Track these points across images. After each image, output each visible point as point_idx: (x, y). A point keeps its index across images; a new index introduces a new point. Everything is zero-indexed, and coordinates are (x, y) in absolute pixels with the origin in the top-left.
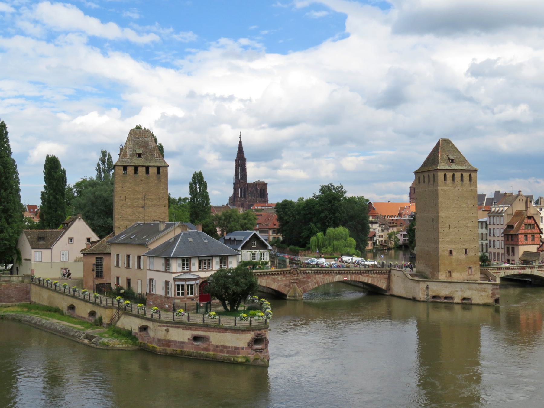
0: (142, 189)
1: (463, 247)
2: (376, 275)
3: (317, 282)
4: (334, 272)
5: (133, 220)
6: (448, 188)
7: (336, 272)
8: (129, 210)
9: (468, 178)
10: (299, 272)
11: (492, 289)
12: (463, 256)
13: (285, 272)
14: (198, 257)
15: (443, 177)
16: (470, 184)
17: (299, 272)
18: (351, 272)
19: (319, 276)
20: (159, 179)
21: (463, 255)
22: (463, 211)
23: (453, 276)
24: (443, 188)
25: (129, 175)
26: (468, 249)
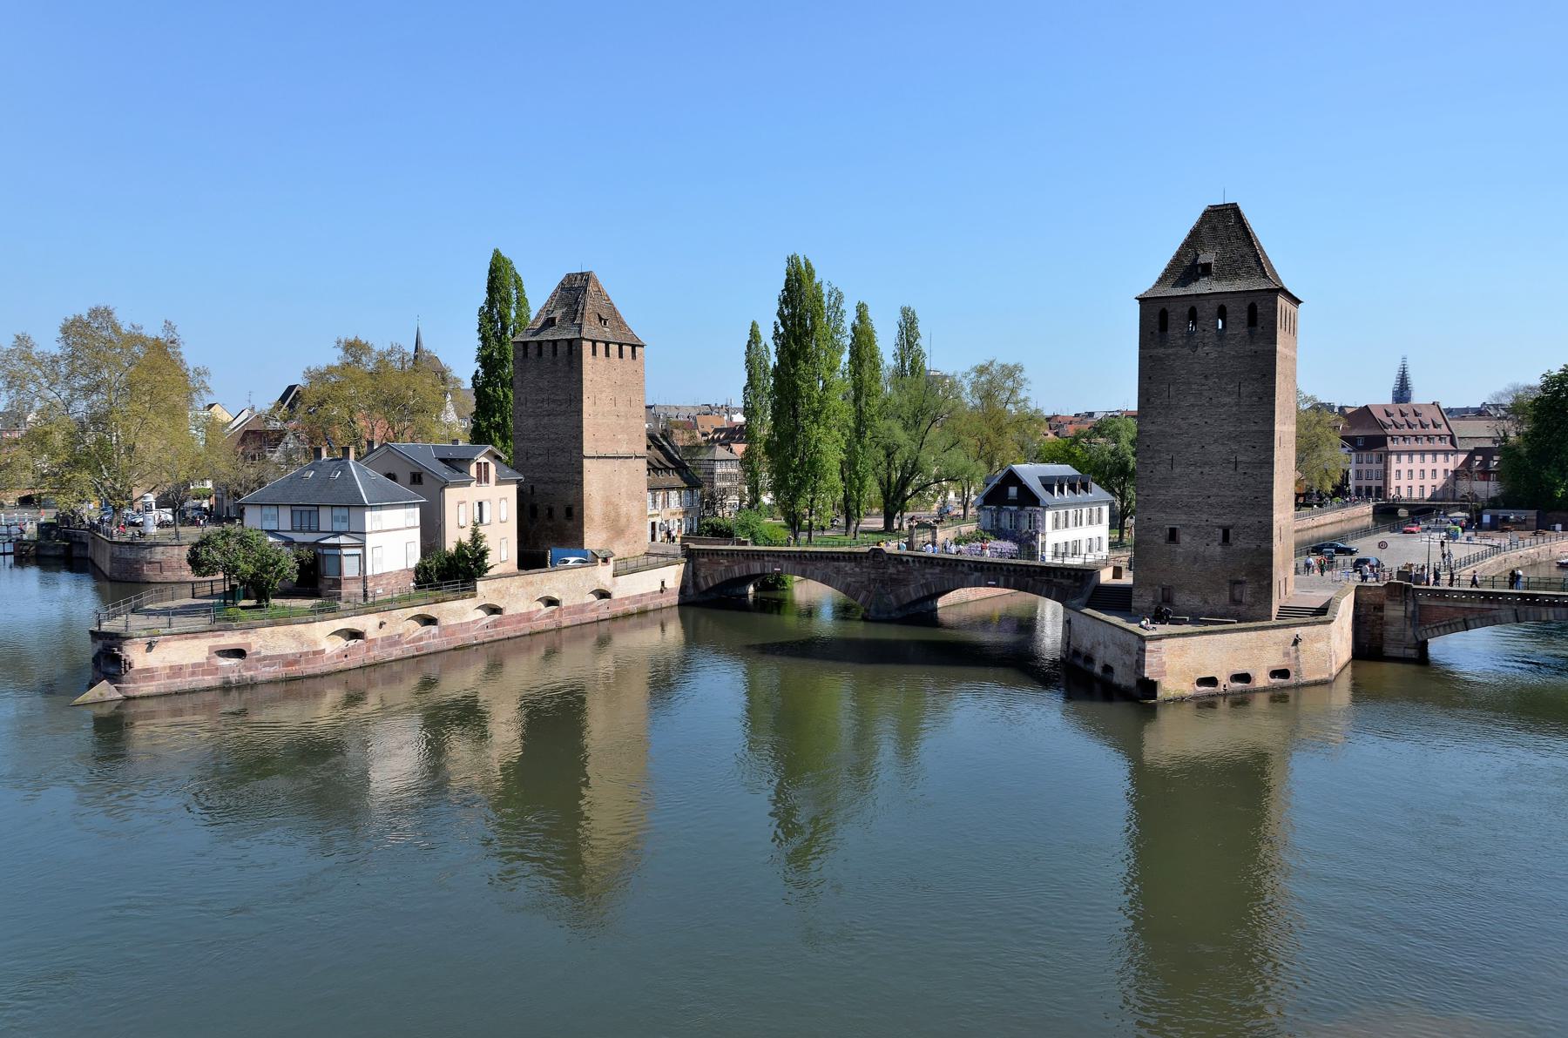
0: (546, 383)
1: (1214, 520)
2: (1071, 581)
3: (926, 585)
4: (963, 565)
5: (535, 440)
6: (1170, 351)
7: (969, 566)
8: (531, 422)
9: (1245, 316)
10: (885, 558)
11: (1137, 649)
12: (1216, 549)
13: (858, 556)
14: (291, 505)
15: (1157, 319)
16: (1250, 332)
17: (885, 558)
18: (1005, 569)
19: (931, 571)
20: (570, 363)
21: (1216, 544)
22: (1224, 417)
23: (1177, 603)
24: (1154, 352)
25: (531, 358)
26: (1232, 527)
